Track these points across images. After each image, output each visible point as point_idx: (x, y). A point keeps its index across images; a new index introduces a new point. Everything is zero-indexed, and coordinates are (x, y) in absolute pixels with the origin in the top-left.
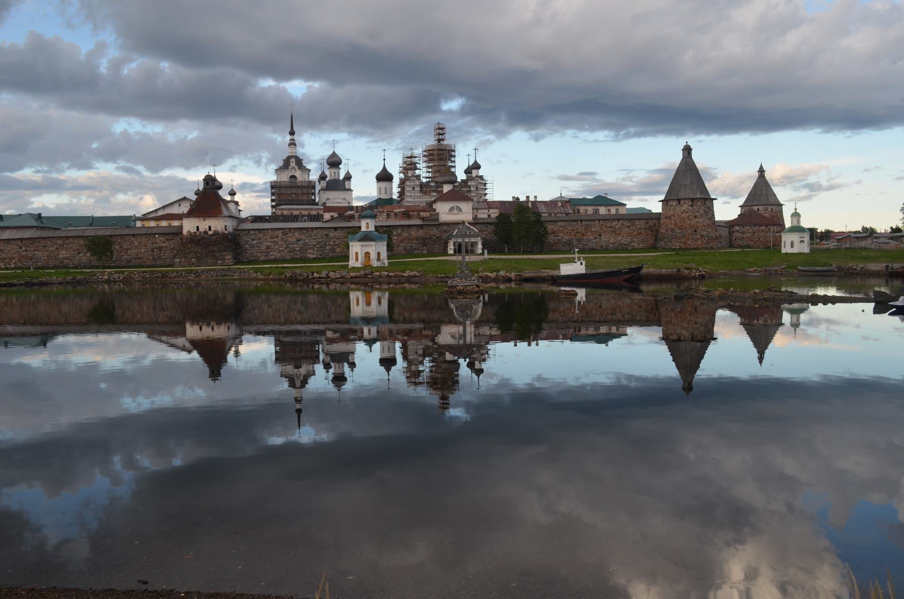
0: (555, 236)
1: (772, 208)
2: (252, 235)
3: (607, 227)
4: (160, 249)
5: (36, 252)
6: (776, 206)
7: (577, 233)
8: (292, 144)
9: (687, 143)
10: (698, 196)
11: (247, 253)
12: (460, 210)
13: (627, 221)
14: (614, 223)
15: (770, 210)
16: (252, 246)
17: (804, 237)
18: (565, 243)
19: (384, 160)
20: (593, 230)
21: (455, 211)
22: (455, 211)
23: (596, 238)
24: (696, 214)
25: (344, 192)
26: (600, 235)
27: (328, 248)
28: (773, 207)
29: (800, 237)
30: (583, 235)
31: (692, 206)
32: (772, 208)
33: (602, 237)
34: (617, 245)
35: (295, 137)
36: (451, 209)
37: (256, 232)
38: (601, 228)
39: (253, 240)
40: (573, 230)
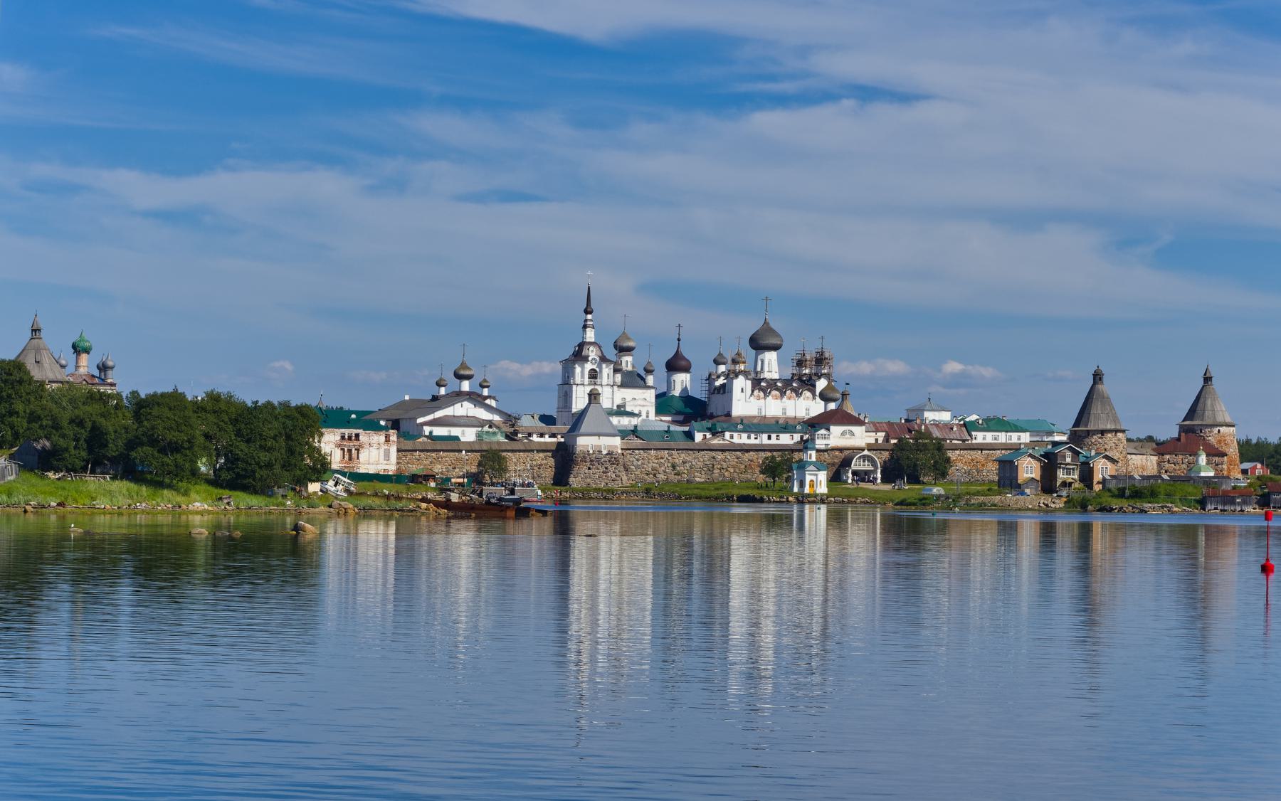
2: (636, 455)
4: (540, 466)
7: (977, 462)
10: (1109, 427)
11: (632, 474)
12: (852, 434)
16: (637, 467)
19: (679, 340)
21: (848, 436)
22: (848, 436)
24: (1106, 446)
25: (644, 391)
30: (983, 465)
32: (1219, 431)
36: (843, 434)
37: (641, 451)
39: (638, 460)
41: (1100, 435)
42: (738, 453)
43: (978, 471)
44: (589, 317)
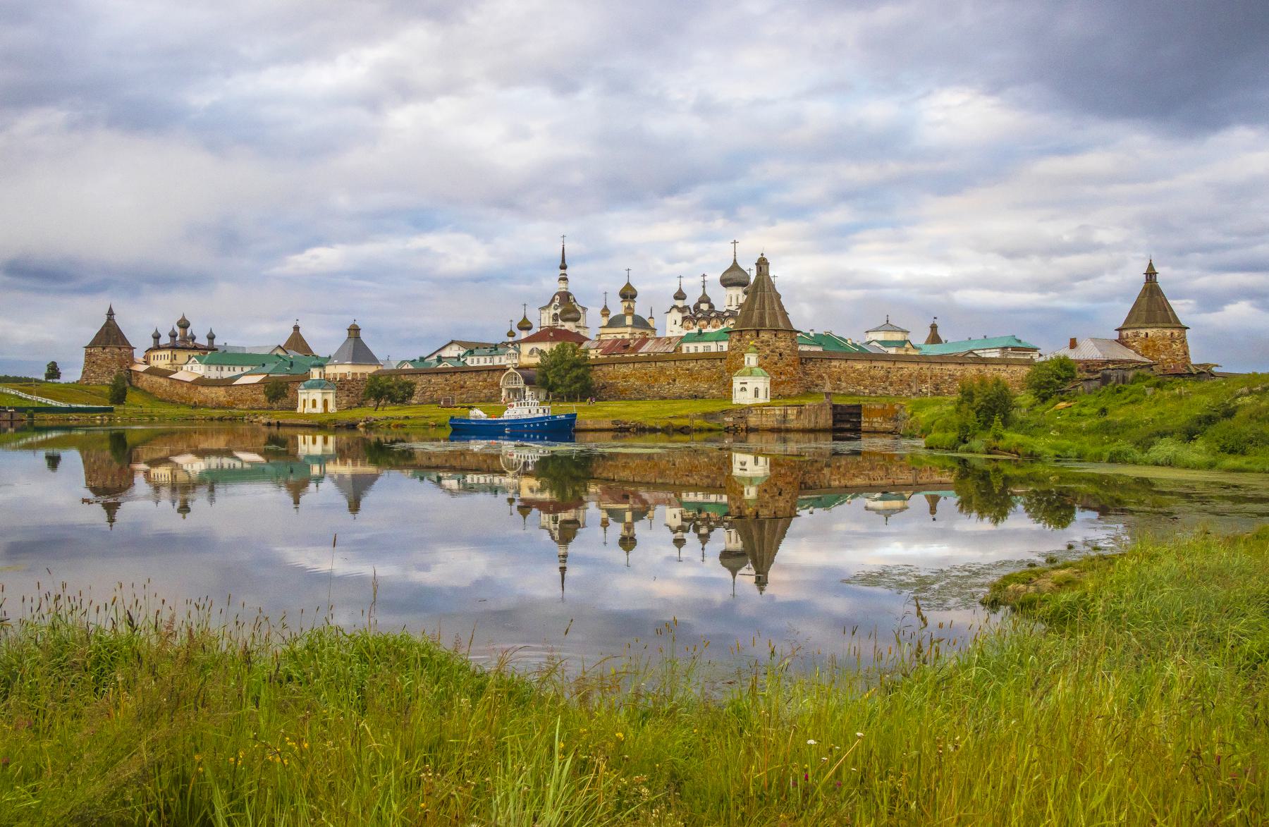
0: (625, 382)
1: (1147, 334)
3: (683, 370)
6: (1155, 330)
8: (564, 279)
9: (762, 255)
13: (706, 362)
14: (691, 365)
15: (1143, 336)
17: (746, 383)
18: (635, 390)
20: (668, 373)
22: (535, 354)
23: (669, 384)
26: (674, 380)
27: (427, 394)
28: (1149, 331)
29: (741, 383)
30: (656, 380)
31: (739, 340)
33: (677, 382)
34: (691, 392)
35: (567, 272)
38: (676, 371)
40: (646, 374)
41: (738, 337)
42: (448, 376)
43: (649, 387)
44: (563, 271)
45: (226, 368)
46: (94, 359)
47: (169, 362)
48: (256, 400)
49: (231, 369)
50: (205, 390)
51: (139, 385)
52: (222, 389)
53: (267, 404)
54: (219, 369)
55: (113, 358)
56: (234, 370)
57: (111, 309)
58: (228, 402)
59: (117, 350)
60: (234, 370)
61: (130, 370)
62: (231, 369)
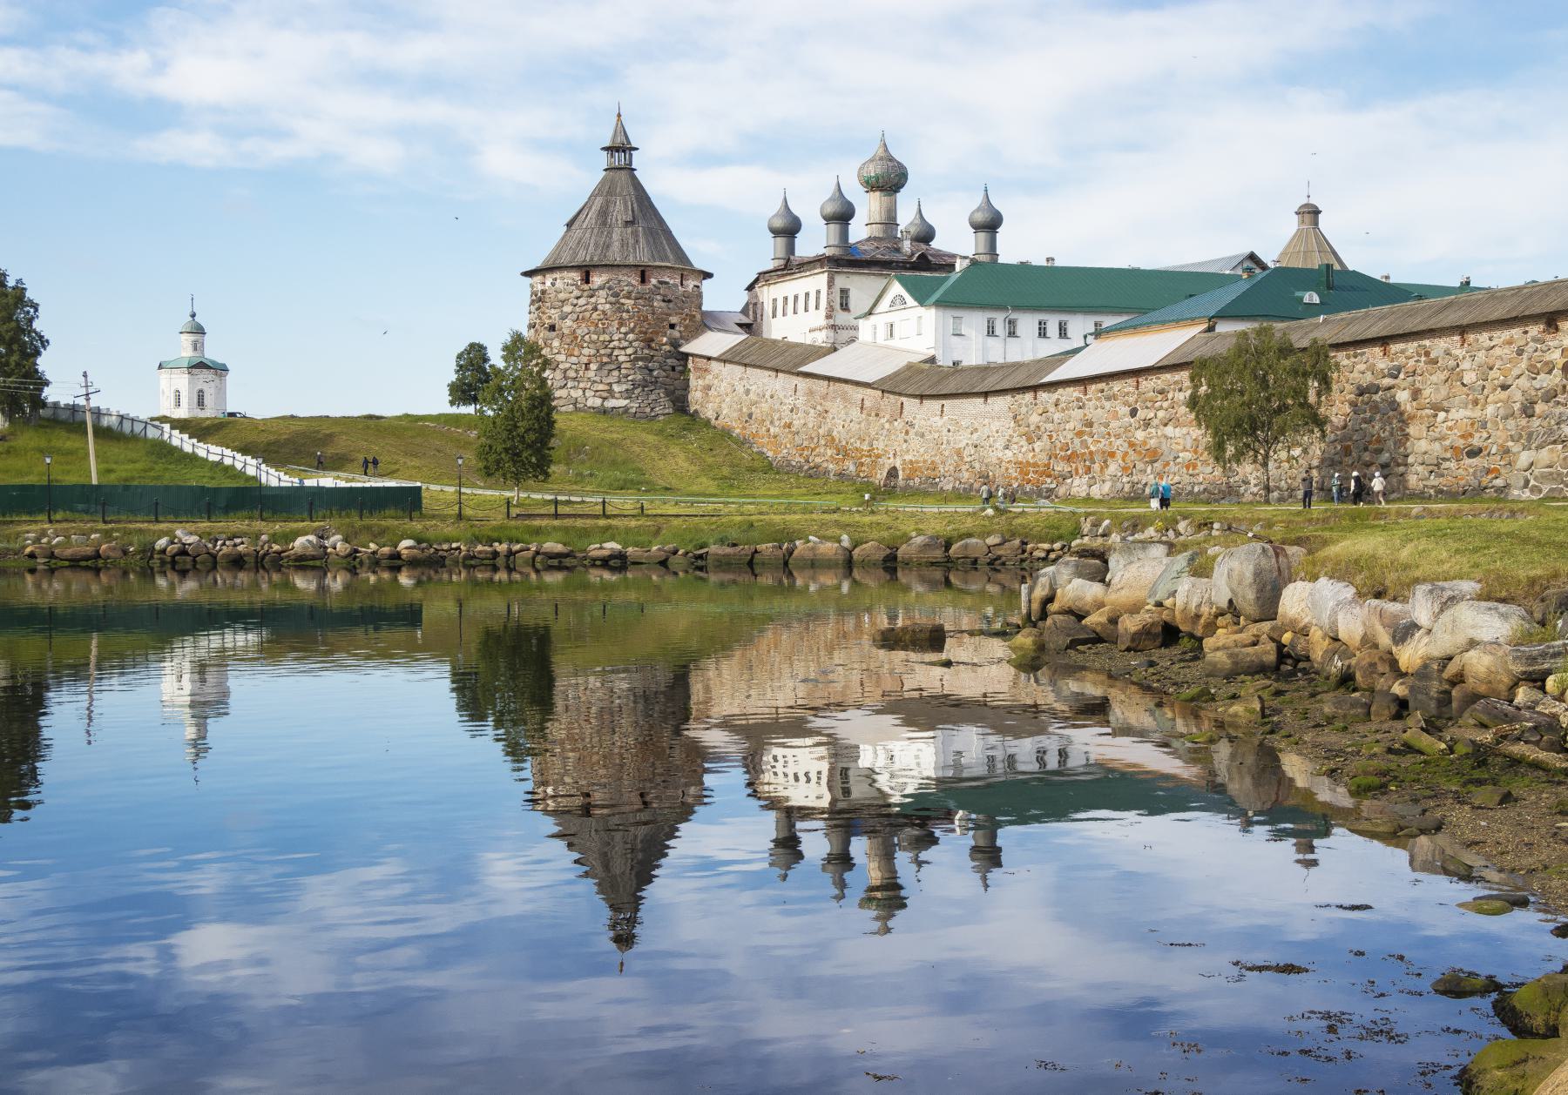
5: (1169, 430)
45: (1027, 323)
46: (554, 314)
47: (818, 318)
48: (1153, 456)
49: (1053, 329)
50: (925, 414)
51: (709, 413)
52: (1000, 403)
53: (1209, 473)
54: (1000, 329)
55: (620, 308)
56: (1063, 332)
57: (621, 129)
58: (1023, 467)
59: (634, 280)
60: (1063, 332)
61: (686, 356)
62: (1053, 329)
